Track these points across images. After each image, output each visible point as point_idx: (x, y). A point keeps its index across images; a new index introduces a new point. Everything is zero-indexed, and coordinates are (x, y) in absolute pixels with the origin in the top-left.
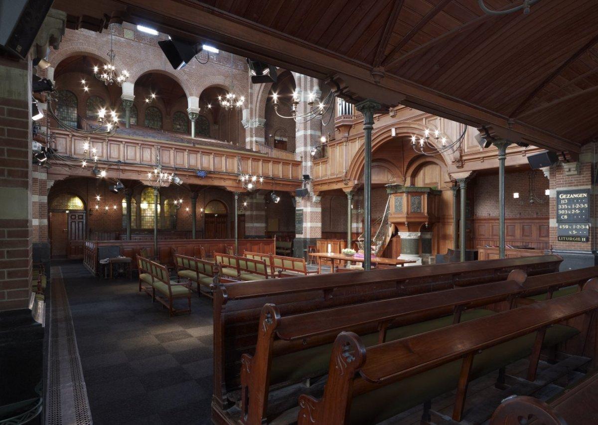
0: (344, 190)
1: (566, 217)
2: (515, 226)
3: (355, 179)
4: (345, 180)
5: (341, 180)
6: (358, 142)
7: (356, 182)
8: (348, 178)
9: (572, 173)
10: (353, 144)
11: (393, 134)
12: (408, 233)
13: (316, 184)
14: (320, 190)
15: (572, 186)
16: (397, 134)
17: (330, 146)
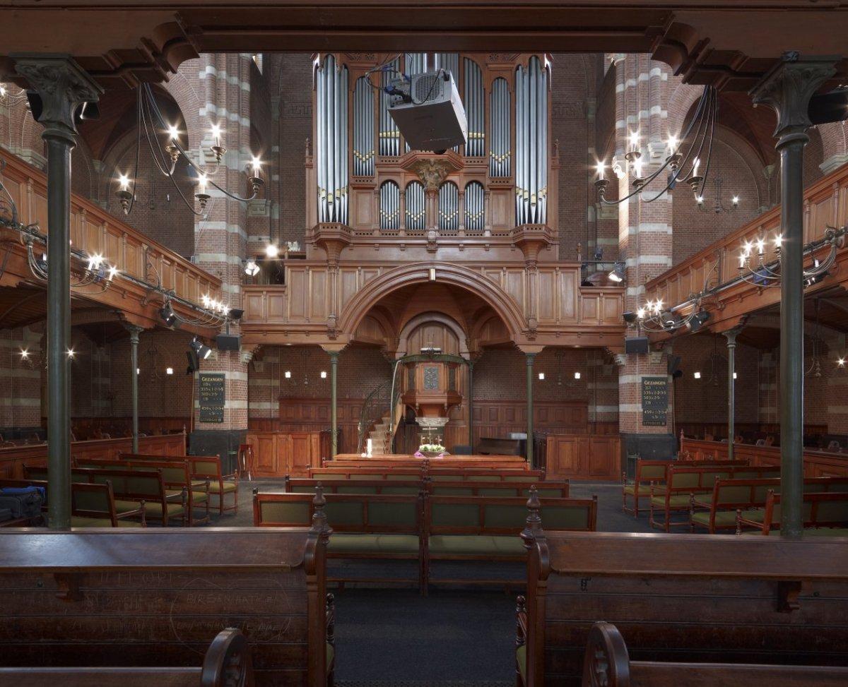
0: (325, 347)
1: (650, 402)
2: (514, 410)
3: (350, 333)
4: (333, 332)
5: (326, 329)
6: (360, 274)
7: (352, 337)
8: (339, 329)
9: (657, 361)
10: (349, 277)
11: (433, 277)
12: (440, 419)
13: (247, 329)
14: (263, 342)
15: (653, 373)
16: (436, 278)
17: (289, 267)
